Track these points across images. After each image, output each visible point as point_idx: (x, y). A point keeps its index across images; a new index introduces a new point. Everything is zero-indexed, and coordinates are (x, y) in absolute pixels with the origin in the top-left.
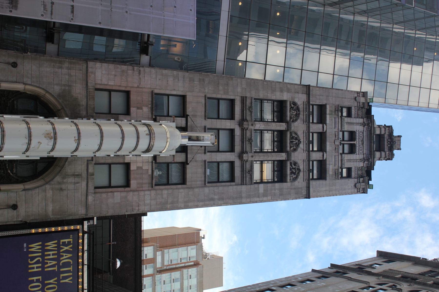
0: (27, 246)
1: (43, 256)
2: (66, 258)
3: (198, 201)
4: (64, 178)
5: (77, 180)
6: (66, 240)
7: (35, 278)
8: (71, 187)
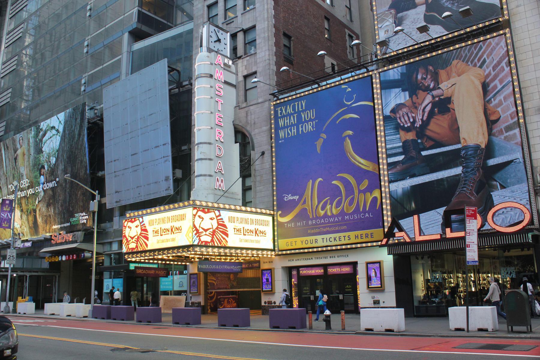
0: (281, 140)
1: (287, 127)
2: (290, 110)
3: (264, 10)
4: (248, 123)
5: (249, 114)
6: (279, 112)
7: (300, 129)
8: (253, 116)
